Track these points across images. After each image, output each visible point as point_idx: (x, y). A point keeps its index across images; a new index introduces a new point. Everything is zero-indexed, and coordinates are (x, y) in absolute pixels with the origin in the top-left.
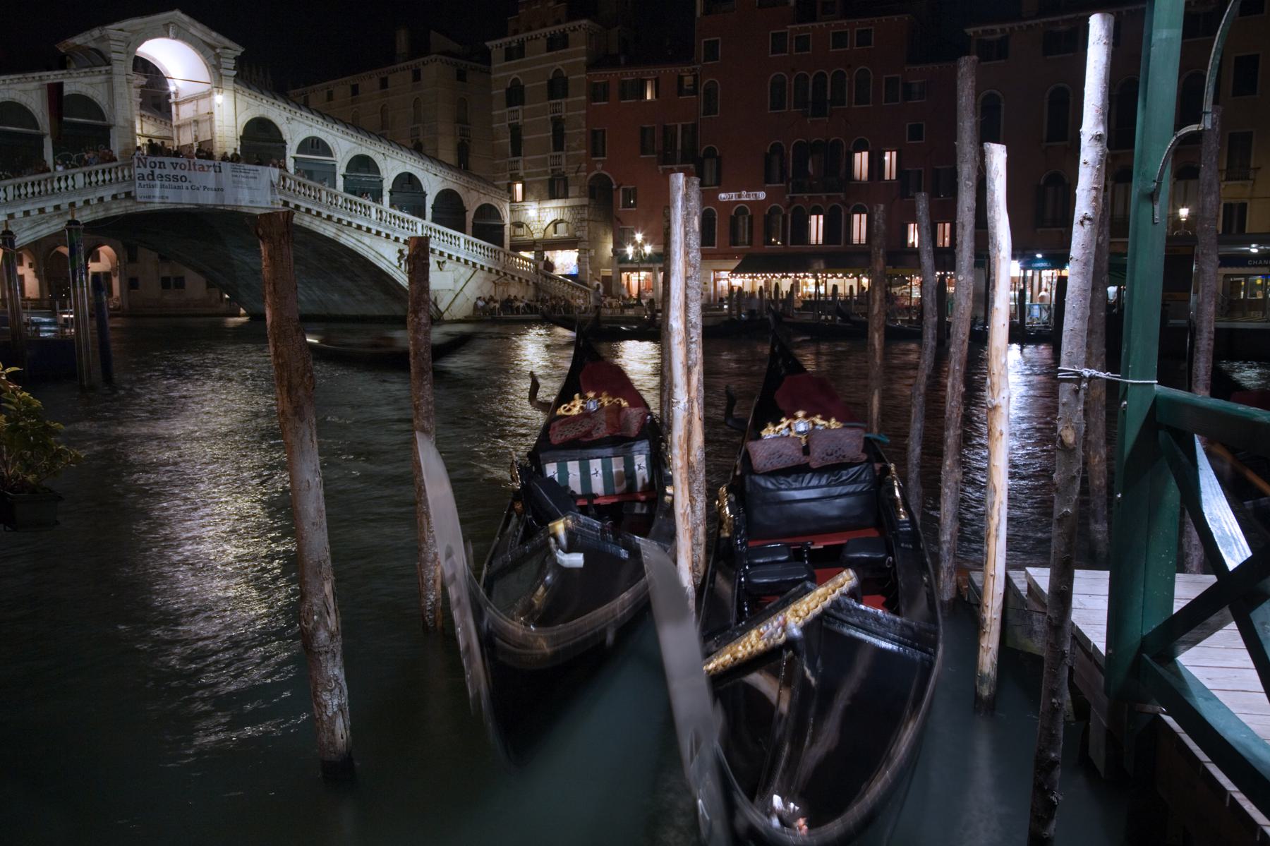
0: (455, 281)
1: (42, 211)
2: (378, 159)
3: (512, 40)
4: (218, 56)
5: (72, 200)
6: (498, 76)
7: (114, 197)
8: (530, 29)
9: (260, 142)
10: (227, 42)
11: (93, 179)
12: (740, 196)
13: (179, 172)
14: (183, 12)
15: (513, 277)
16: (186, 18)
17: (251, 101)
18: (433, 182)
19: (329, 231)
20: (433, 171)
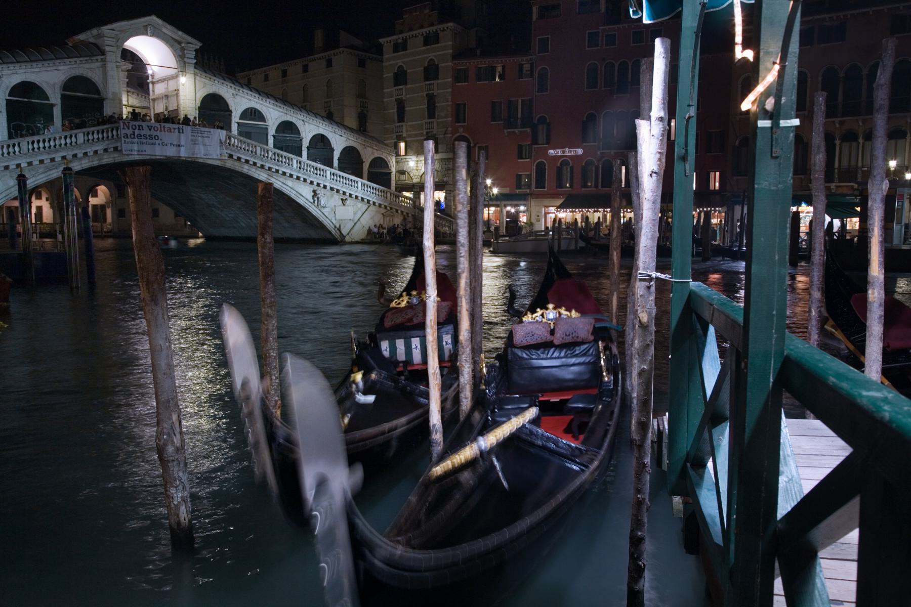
0: (355, 213)
1: (52, 160)
2: (299, 124)
3: (398, 38)
4: (183, 49)
5: (75, 152)
6: (388, 64)
7: (106, 150)
8: (411, 30)
9: (213, 110)
10: (189, 39)
11: (90, 137)
12: (564, 152)
13: (153, 133)
14: (158, 17)
15: (397, 211)
16: (160, 21)
17: (207, 81)
18: (339, 141)
19: (262, 176)
20: (339, 132)
